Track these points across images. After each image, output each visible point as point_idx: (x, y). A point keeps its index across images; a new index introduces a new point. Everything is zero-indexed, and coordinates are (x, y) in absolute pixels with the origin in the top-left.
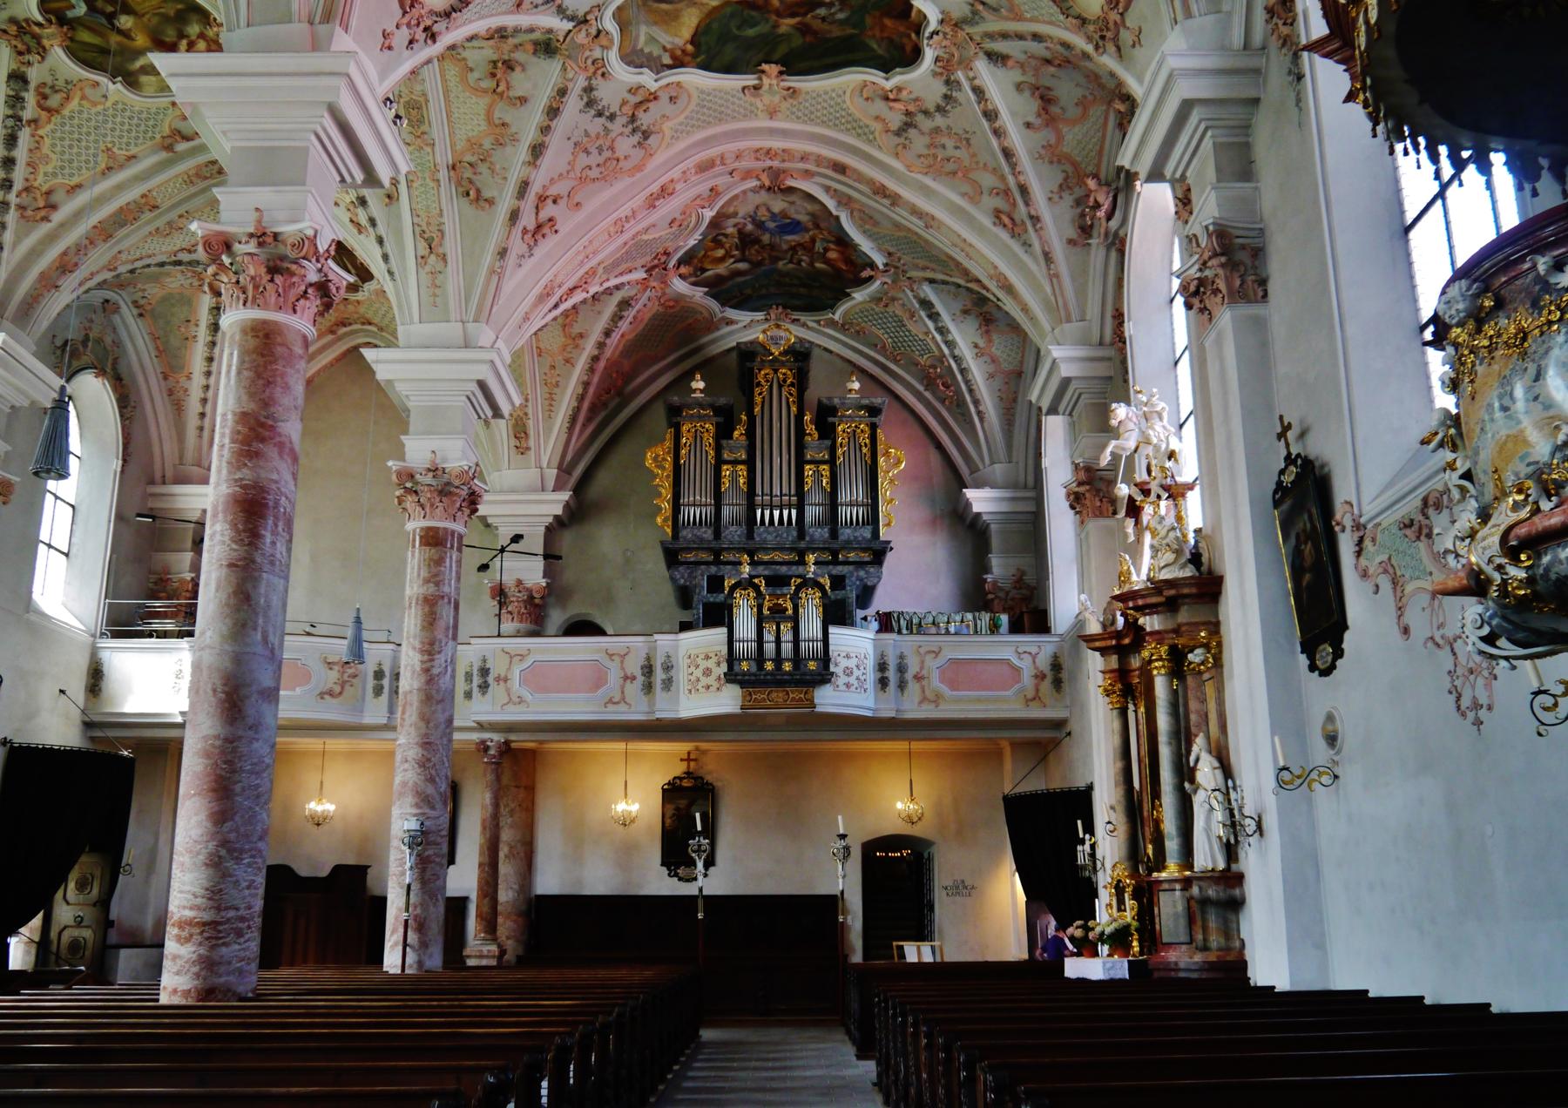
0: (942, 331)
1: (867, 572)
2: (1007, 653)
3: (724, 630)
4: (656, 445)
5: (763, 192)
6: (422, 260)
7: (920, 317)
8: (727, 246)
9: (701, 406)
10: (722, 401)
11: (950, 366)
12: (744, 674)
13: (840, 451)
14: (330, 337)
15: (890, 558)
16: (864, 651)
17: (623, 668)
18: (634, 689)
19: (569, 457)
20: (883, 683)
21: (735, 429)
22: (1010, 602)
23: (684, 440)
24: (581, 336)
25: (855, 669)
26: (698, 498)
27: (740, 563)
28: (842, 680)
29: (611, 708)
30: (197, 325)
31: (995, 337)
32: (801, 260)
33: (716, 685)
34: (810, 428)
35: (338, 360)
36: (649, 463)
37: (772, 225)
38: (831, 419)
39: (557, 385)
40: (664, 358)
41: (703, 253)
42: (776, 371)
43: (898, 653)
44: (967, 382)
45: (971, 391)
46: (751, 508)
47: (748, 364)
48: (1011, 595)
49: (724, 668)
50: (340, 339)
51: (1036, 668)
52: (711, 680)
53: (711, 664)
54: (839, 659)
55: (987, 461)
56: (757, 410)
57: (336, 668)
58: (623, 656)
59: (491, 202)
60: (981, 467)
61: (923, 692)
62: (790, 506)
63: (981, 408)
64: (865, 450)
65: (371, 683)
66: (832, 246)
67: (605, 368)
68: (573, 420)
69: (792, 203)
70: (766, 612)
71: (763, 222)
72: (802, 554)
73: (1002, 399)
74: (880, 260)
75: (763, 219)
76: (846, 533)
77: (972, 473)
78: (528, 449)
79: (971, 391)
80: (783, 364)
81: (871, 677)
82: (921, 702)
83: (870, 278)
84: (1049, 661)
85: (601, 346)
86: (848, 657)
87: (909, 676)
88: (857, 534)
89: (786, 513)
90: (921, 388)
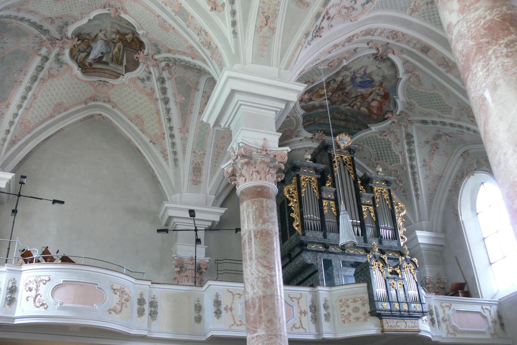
0: (411, 151)
3: (365, 285)
6: (258, 29)
9: (309, 167)
14: (83, 106)
17: (299, 307)
18: (307, 320)
19: (220, 191)
21: (326, 183)
29: (295, 330)
30: (25, 75)
31: (435, 156)
32: (355, 105)
33: (363, 317)
34: (361, 188)
35: (81, 121)
44: (414, 180)
50: (86, 109)
55: (417, 220)
57: (118, 293)
59: (308, 5)
63: (419, 193)
65: (136, 306)
66: (379, 98)
69: (379, 68)
73: (429, 189)
74: (400, 108)
76: (386, 243)
78: (200, 182)
79: (415, 184)
84: (496, 313)
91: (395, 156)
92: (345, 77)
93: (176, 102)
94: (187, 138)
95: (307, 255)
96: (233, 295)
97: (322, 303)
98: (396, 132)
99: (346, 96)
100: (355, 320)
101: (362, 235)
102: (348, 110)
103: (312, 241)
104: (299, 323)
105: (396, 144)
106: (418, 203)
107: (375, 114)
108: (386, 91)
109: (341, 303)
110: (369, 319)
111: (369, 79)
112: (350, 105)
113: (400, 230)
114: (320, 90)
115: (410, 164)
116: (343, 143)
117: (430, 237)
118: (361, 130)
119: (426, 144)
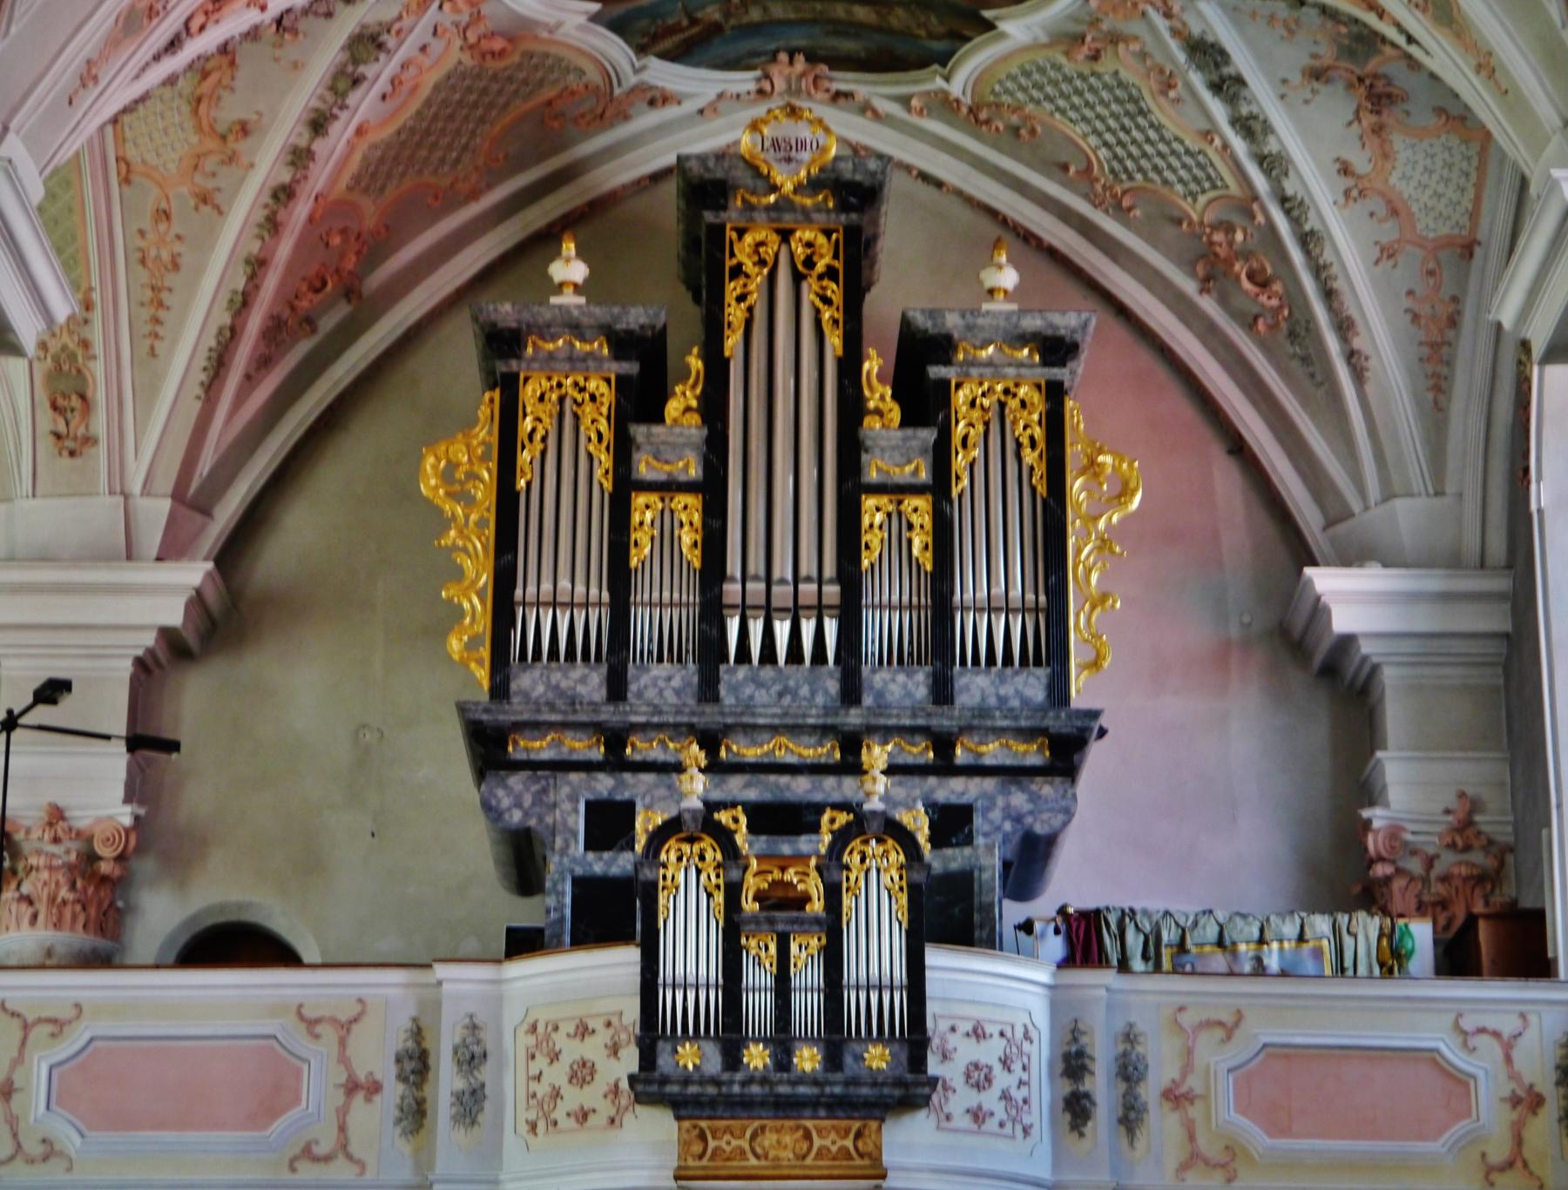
0: (1250, 127)
1: (1034, 798)
2: (1434, 1035)
4: (449, 437)
9: (576, 329)
10: (636, 317)
11: (1271, 227)
12: (686, 1081)
13: (960, 462)
15: (1096, 757)
16: (1020, 1020)
17: (344, 1060)
20: (1077, 1109)
21: (664, 396)
22: (1438, 889)
23: (528, 424)
24: (244, 129)
26: (564, 583)
27: (679, 768)
28: (960, 1099)
31: (1398, 142)
33: (605, 1109)
34: (879, 395)
36: (430, 485)
38: (935, 371)
39: (176, 266)
40: (474, 195)
42: (785, 235)
43: (1120, 1025)
45: (1329, 294)
46: (712, 611)
47: (709, 217)
48: (1439, 869)
49: (630, 1060)
51: (1514, 1076)
52: (592, 1095)
53: (593, 1049)
54: (954, 1041)
56: (732, 343)
58: (346, 1027)
60: (1356, 506)
61: (1192, 1137)
62: (820, 610)
63: (1357, 343)
64: (1030, 457)
67: (311, 219)
68: (219, 363)
70: (750, 906)
72: (852, 744)
73: (1416, 318)
76: (973, 687)
77: (1330, 523)
78: (90, 440)
79: (1329, 294)
80: (806, 217)
81: (1043, 1092)
82: (1184, 1167)
85: (300, 157)
86: (978, 1033)
87: (1149, 1092)
88: (1007, 690)
89: (808, 628)
90: (1189, 286)
95: (506, 787)
96: (26, 1027)
100: (572, 1123)
101: (837, 660)
103: (525, 717)
105: (1164, 93)
109: (531, 1040)
116: (789, 160)
117: (1413, 598)
118: (968, 39)
119: (1316, 85)
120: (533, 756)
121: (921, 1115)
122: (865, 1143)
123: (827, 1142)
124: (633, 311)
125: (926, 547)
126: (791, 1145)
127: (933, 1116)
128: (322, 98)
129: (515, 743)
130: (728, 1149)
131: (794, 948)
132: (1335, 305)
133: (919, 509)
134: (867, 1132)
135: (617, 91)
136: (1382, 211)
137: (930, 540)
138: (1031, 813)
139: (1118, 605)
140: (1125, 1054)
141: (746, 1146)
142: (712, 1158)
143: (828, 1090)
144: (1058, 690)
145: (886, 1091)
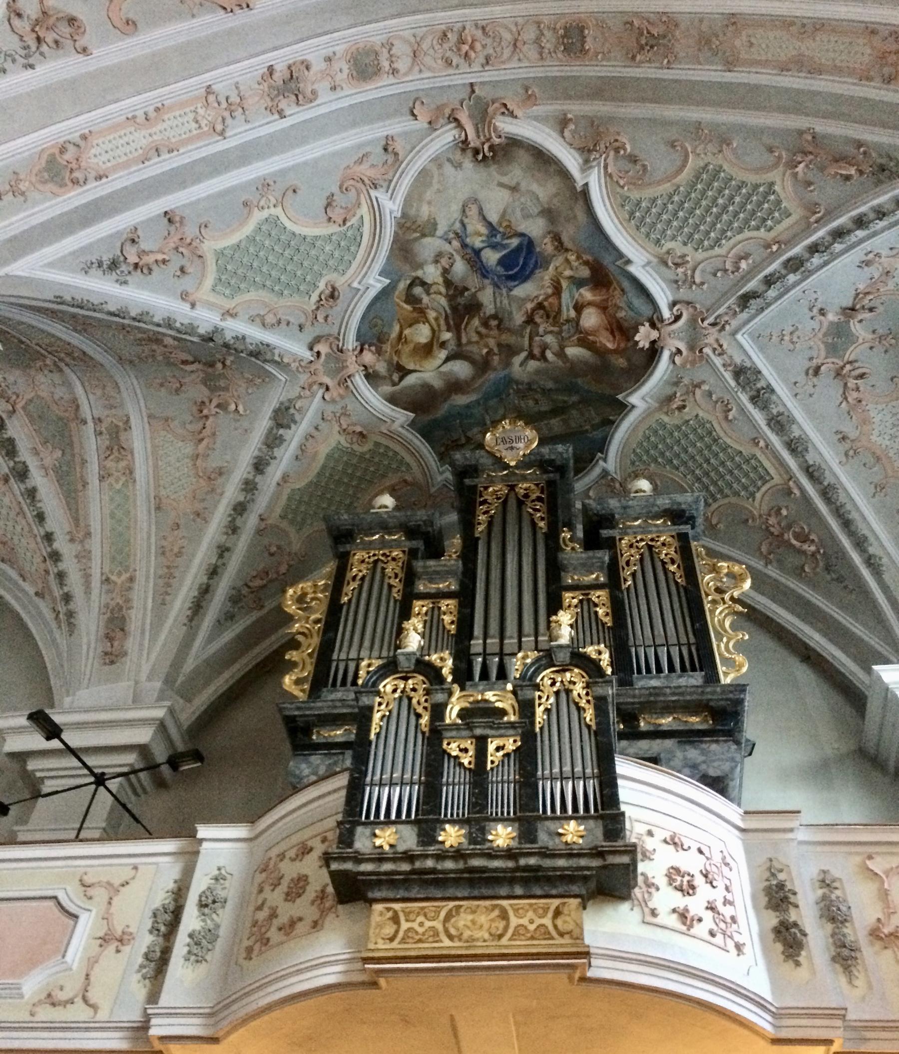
0: (779, 423)
1: (704, 753)
5: (468, 164)
7: (742, 410)
8: (432, 315)
9: (384, 526)
25: (699, 881)
29: (46, 1014)
32: (544, 347)
37: (491, 257)
41: (397, 328)
42: (512, 488)
44: (839, 512)
45: (846, 524)
47: (467, 481)
52: (303, 907)
63: (871, 550)
64: (673, 568)
66: (587, 294)
68: (198, 607)
71: (477, 252)
74: (662, 295)
75: (478, 243)
79: (846, 524)
80: (524, 478)
83: (653, 352)
85: (249, 487)
91: (747, 461)
92: (444, 262)
93: (43, 467)
94: (90, 552)
97: (200, 884)
98: (704, 382)
99: (498, 327)
102: (538, 372)
104: (84, 976)
106: (885, 589)
107: (615, 351)
108: (586, 257)
110: (331, 916)
111: (515, 242)
112: (531, 356)
113: (720, 640)
114: (407, 332)
115: (800, 466)
116: (512, 448)
118: (613, 422)
119: (815, 380)
120: (330, 740)
121: (625, 907)
122: (565, 922)
123: (524, 921)
124: (419, 513)
125: (607, 614)
126: (486, 926)
127: (637, 909)
128: (260, 450)
129: (318, 732)
130: (421, 930)
131: (491, 747)
132: (853, 528)
133: (600, 596)
134: (565, 910)
135: (433, 490)
136: (871, 460)
137: (609, 611)
138: (704, 762)
139: (747, 637)
140: (824, 898)
141: (439, 926)
142: (403, 941)
143: (523, 862)
144: (712, 677)
145: (583, 862)
